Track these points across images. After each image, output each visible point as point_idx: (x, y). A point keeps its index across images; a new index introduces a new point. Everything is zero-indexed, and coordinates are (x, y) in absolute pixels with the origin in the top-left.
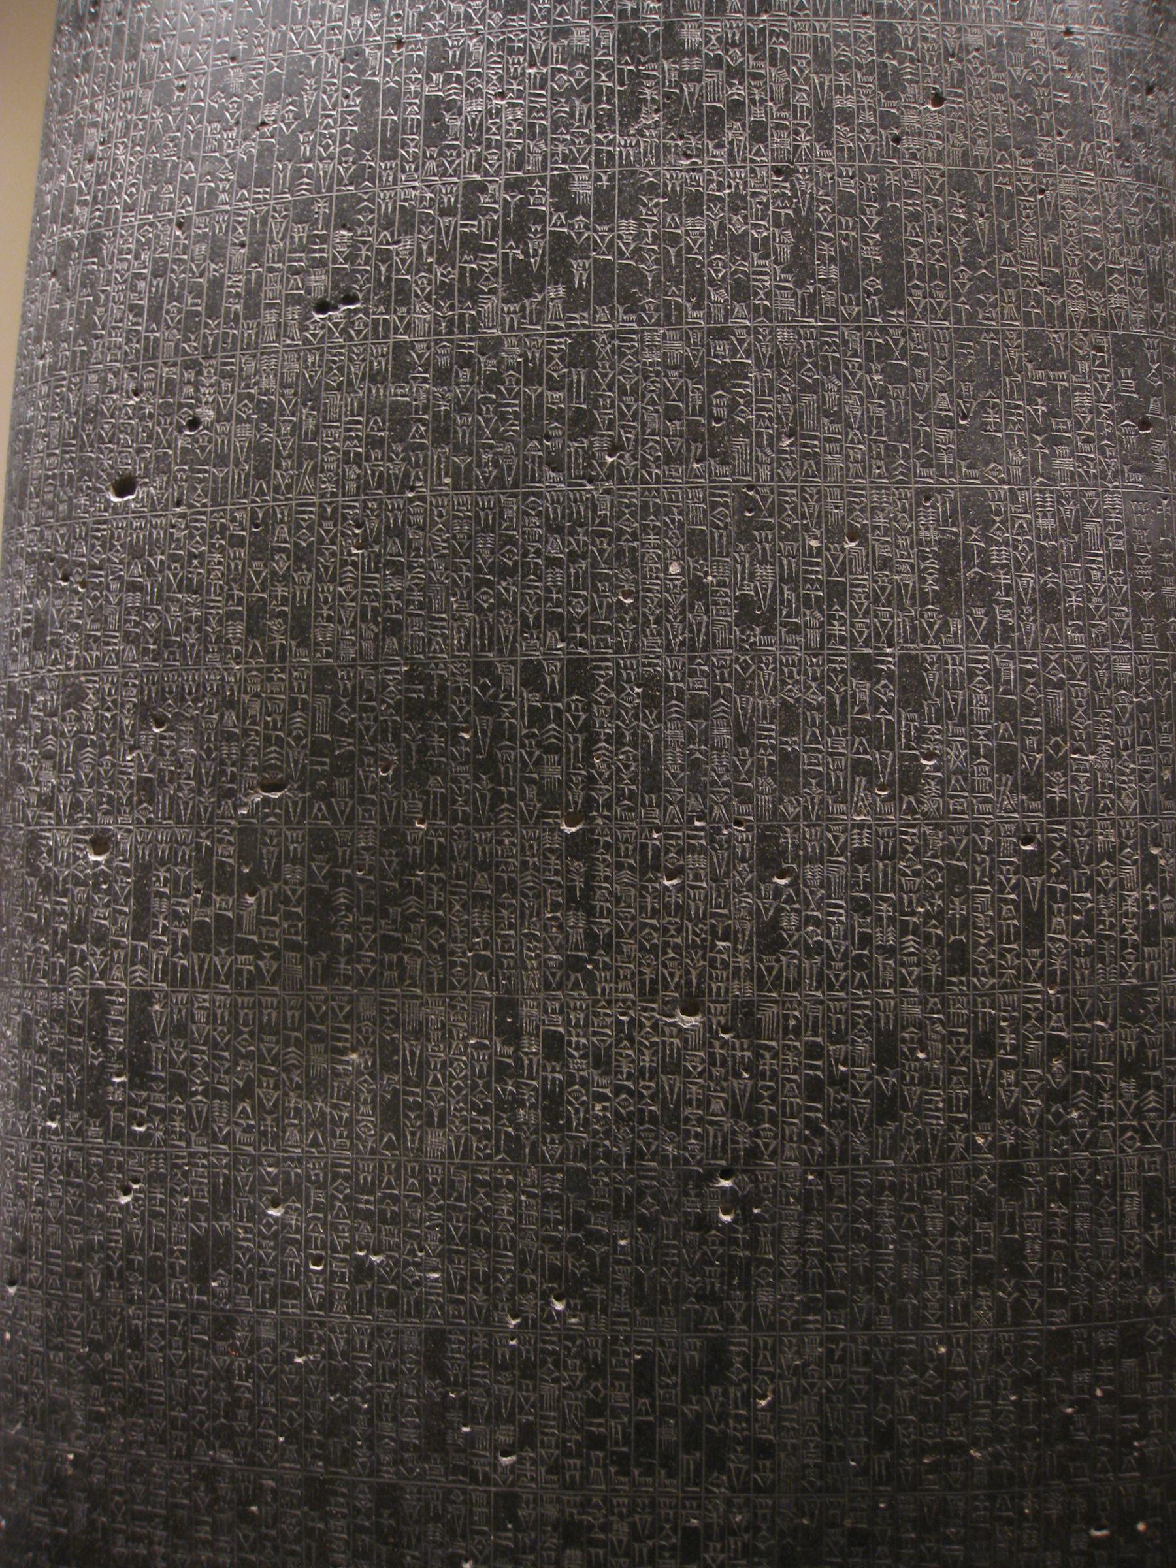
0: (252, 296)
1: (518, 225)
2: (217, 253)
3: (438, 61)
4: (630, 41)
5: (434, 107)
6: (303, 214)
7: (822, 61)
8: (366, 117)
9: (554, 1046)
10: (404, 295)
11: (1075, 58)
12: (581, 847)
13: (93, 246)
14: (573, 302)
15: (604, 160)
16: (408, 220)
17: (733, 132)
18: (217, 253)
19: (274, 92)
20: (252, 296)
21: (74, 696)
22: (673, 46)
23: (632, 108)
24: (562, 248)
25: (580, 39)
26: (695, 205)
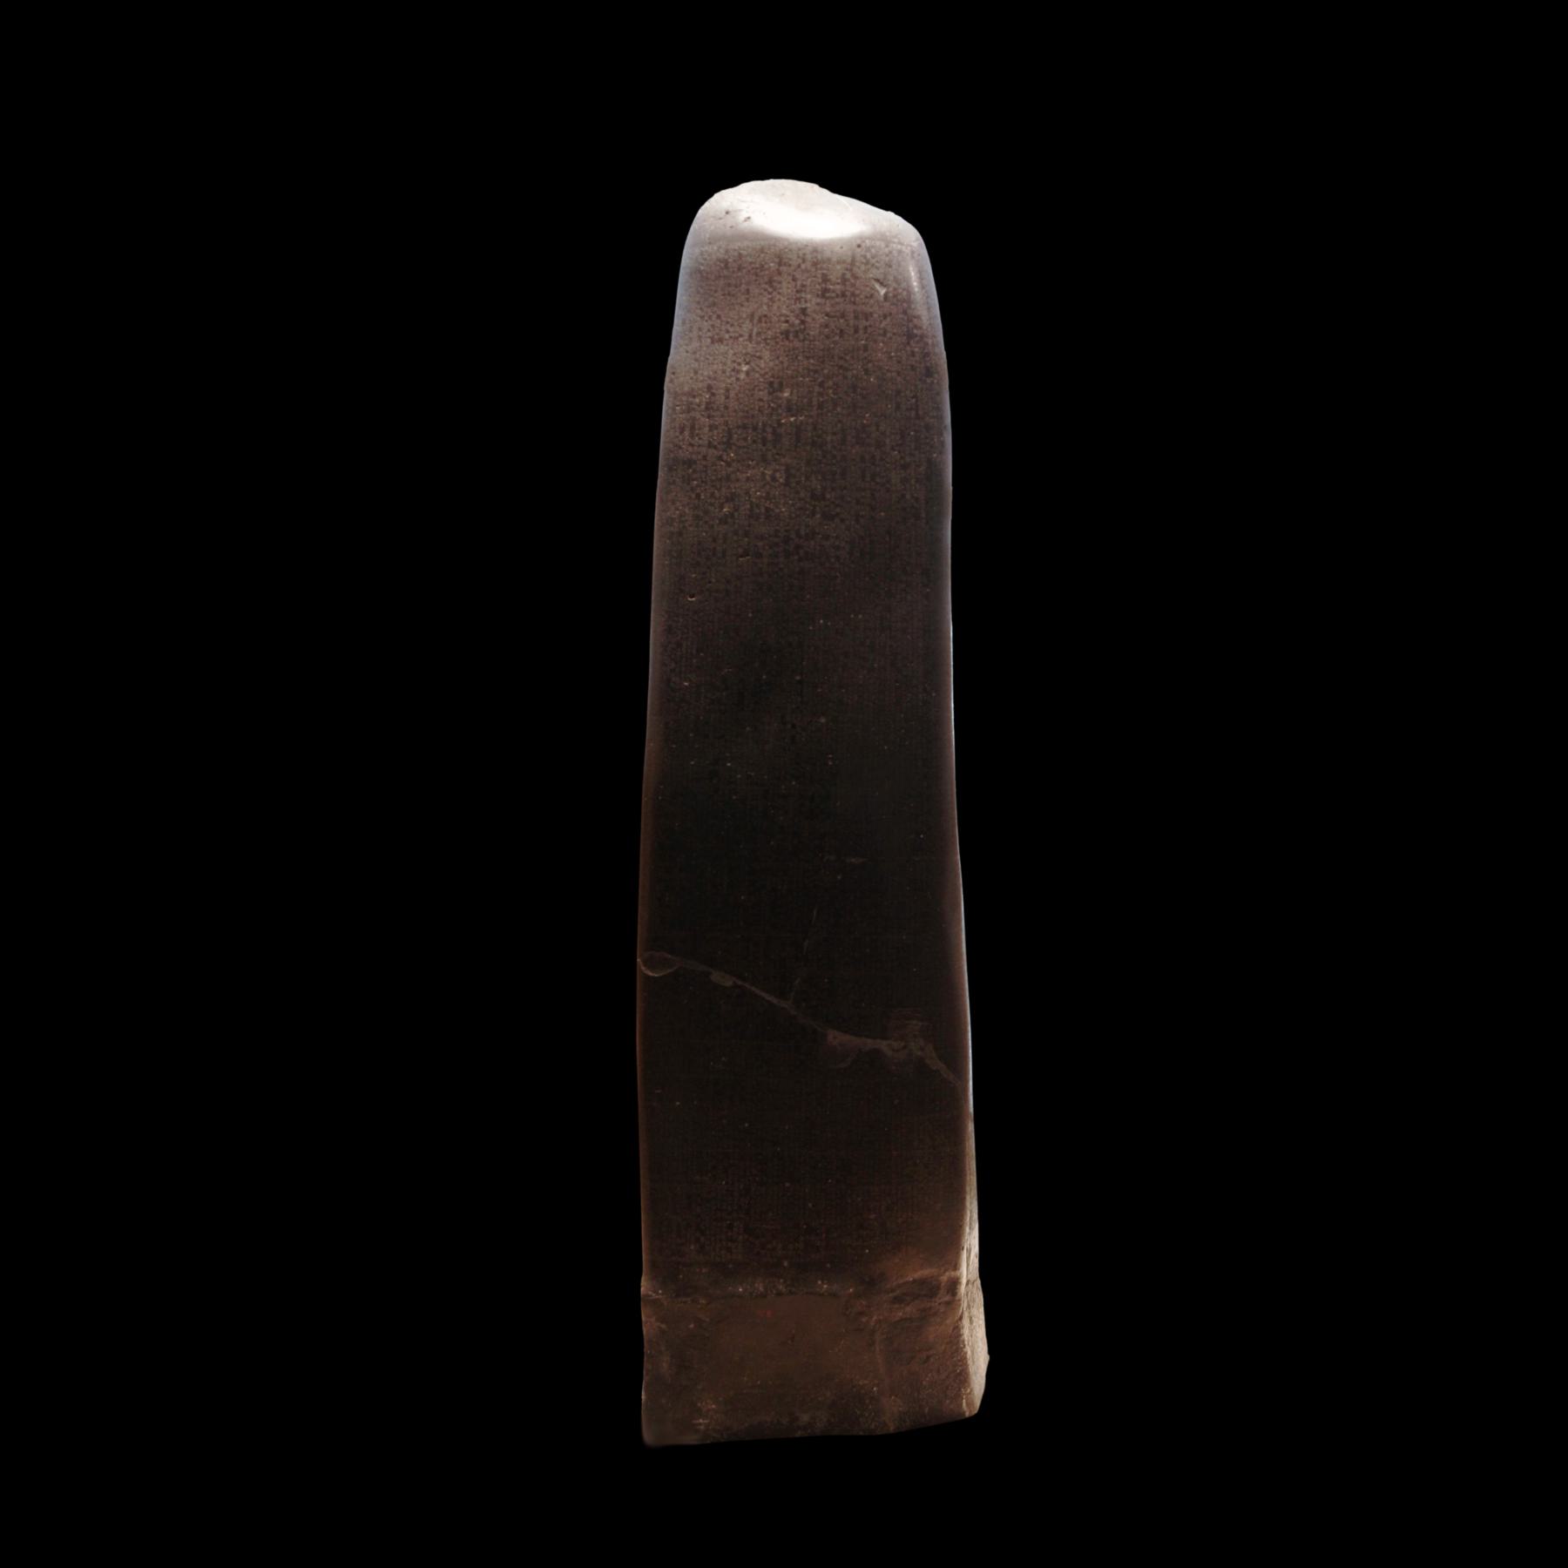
0: (724, 553)
1: (787, 540)
2: (714, 540)
3: (768, 497)
4: (813, 497)
5: (767, 510)
6: (736, 533)
7: (858, 502)
8: (751, 510)
9: (794, 726)
10: (760, 555)
11: (917, 499)
12: (800, 682)
13: (680, 534)
14: (800, 560)
15: (807, 526)
16: (762, 538)
17: (837, 520)
18: (714, 540)
19: (728, 500)
20: (724, 553)
21: (679, 645)
22: (824, 498)
23: (813, 514)
24: (798, 547)
25: (802, 495)
26: (827, 538)
